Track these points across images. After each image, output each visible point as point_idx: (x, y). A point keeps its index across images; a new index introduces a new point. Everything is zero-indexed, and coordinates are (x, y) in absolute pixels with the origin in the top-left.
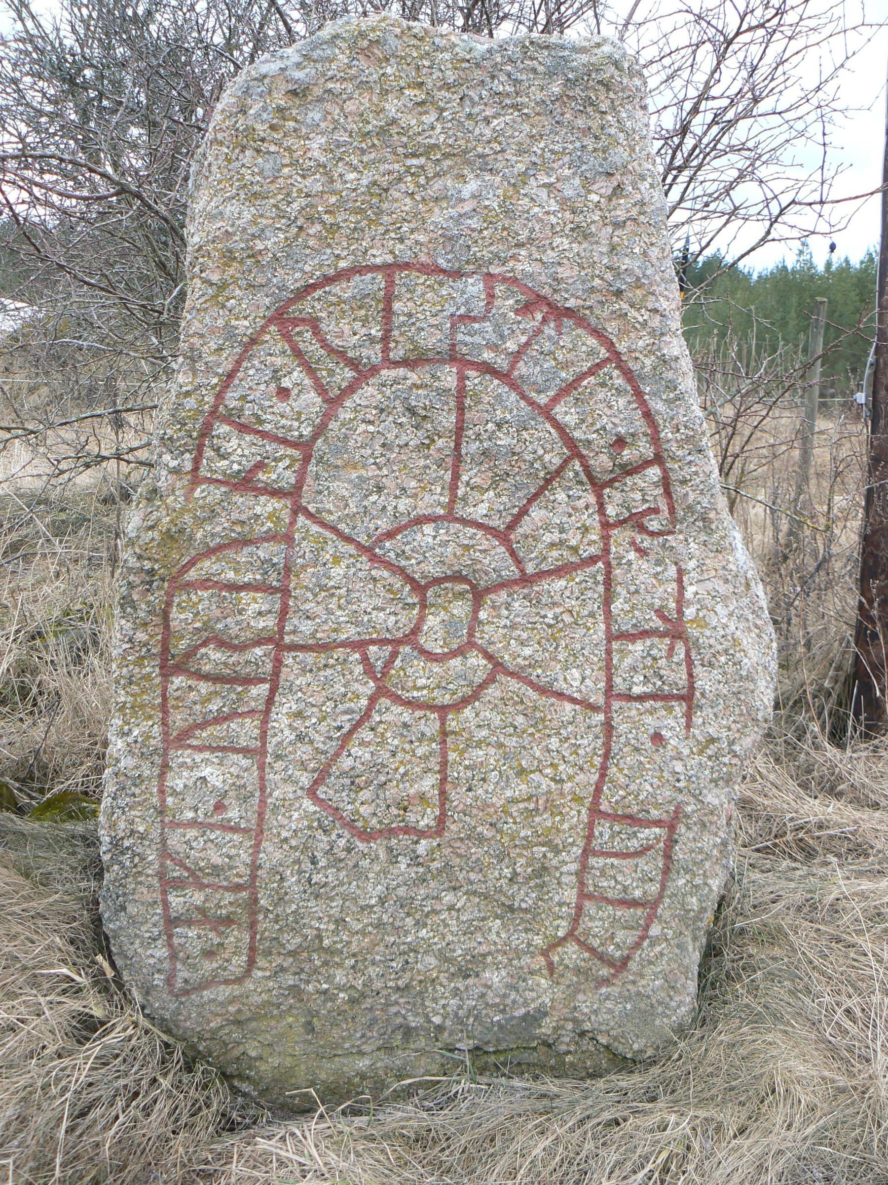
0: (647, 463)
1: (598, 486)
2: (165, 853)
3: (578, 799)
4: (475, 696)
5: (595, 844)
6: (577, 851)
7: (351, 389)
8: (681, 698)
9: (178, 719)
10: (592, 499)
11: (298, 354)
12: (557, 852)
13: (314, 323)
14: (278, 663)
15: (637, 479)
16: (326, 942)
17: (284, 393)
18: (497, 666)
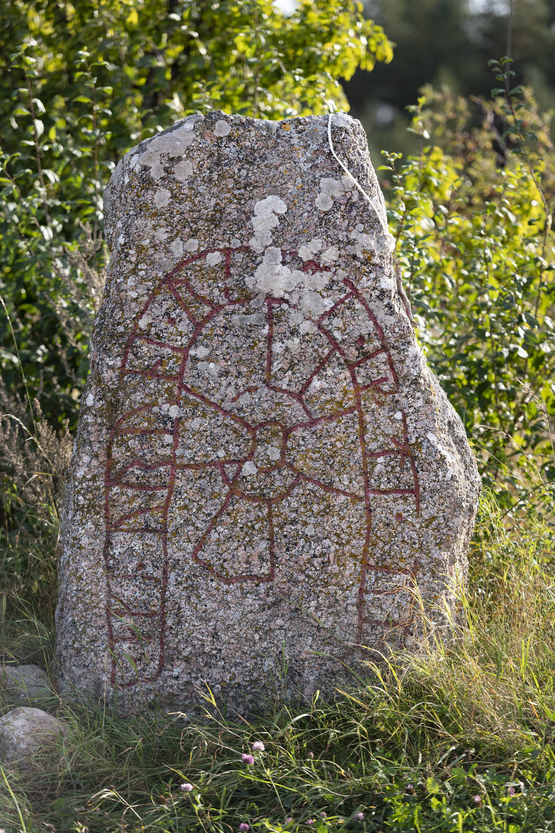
0: (378, 351)
1: (351, 366)
2: (110, 594)
3: (353, 556)
4: (288, 494)
5: (367, 586)
6: (355, 590)
7: (208, 318)
8: (412, 491)
9: (116, 513)
10: (348, 374)
11: (178, 299)
12: (344, 590)
13: (187, 281)
14: (174, 477)
15: (373, 360)
16: (207, 649)
17: (172, 321)
18: (300, 474)
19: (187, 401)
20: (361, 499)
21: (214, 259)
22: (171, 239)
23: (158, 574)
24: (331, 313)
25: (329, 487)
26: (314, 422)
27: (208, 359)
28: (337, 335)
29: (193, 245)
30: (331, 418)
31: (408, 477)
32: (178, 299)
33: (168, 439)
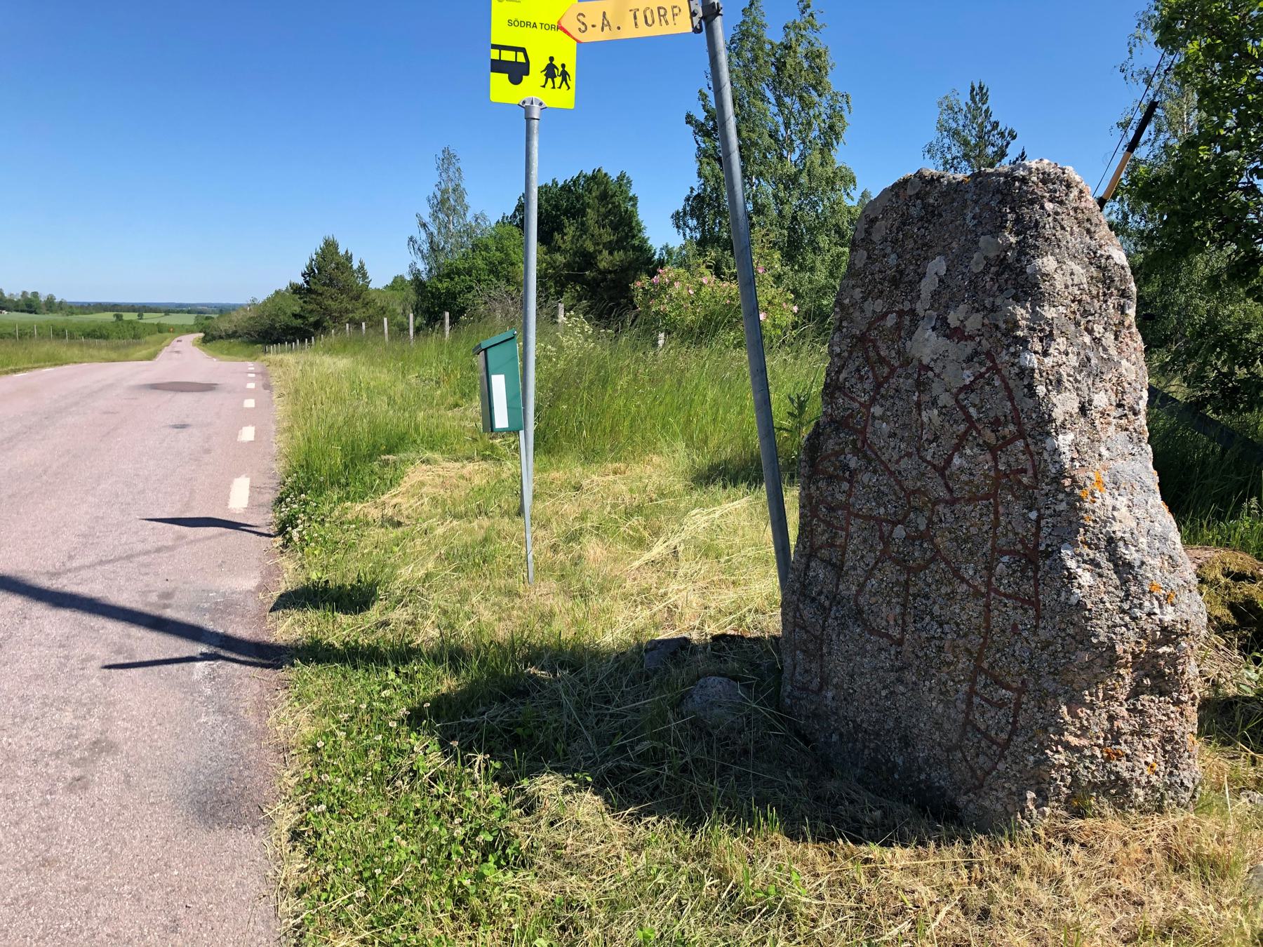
1: (993, 450)
4: (926, 567)
8: (1031, 603)
19: (865, 456)
20: (983, 595)
21: (891, 320)
22: (864, 299)
23: (827, 603)
24: (968, 389)
25: (956, 572)
26: (953, 502)
27: (882, 418)
28: (972, 410)
29: (879, 306)
30: (968, 502)
31: (1028, 587)
32: (867, 359)
33: (845, 486)
